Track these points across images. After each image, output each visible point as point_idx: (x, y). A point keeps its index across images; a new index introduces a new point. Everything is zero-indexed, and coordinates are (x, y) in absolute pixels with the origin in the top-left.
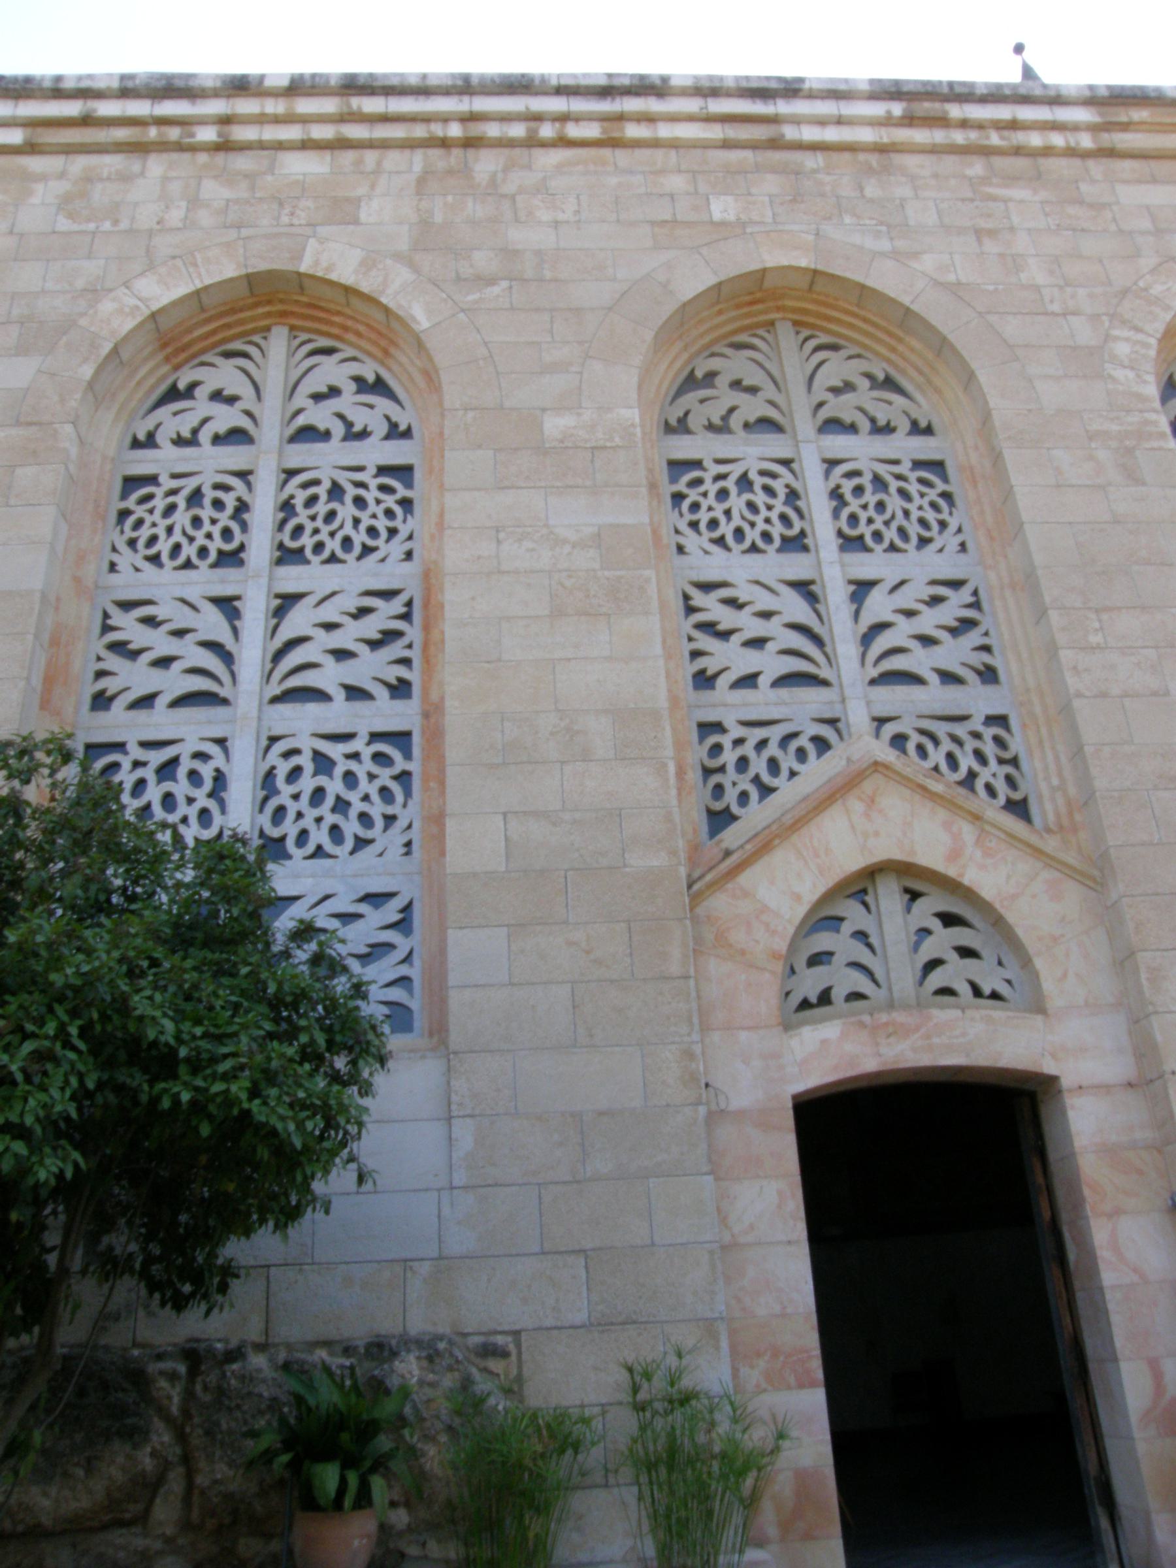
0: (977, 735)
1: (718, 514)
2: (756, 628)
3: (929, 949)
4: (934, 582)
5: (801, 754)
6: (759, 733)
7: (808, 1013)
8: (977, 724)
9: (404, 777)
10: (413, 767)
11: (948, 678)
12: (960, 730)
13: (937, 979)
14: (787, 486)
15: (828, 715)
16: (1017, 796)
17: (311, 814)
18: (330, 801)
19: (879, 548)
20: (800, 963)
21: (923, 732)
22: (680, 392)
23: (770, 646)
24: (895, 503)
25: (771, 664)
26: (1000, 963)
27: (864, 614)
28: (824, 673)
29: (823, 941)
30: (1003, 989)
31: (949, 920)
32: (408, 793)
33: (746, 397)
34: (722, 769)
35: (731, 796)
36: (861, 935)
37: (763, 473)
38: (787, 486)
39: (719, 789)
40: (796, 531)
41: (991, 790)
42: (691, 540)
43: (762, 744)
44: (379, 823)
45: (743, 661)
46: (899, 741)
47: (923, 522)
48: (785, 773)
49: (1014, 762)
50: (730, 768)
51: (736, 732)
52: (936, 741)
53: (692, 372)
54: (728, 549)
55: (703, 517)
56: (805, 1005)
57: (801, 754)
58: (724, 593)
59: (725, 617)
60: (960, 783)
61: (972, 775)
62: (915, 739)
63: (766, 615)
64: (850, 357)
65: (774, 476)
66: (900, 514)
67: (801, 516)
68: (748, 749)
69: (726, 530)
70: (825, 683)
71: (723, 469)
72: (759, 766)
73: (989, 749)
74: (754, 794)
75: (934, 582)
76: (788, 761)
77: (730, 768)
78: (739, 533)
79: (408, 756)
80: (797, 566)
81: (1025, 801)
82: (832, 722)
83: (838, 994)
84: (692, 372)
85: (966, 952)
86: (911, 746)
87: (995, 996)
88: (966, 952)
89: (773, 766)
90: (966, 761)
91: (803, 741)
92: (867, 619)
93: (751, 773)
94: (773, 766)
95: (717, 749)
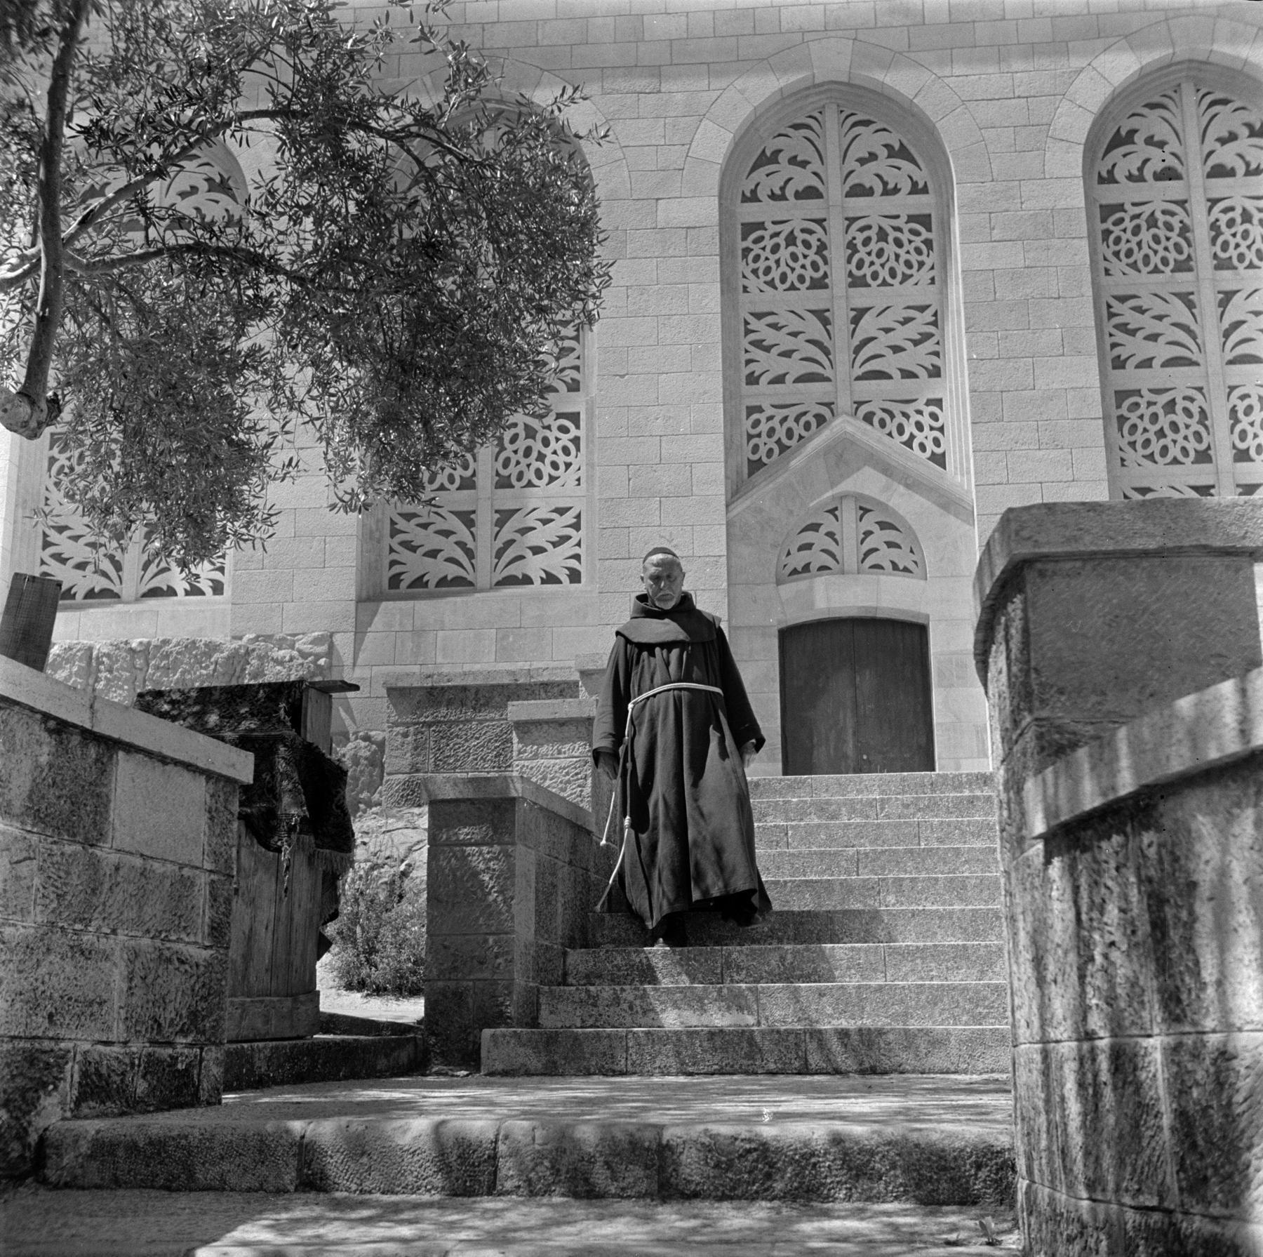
0: (919, 412)
1: (772, 263)
2: (788, 343)
3: (870, 543)
4: (909, 307)
5: (807, 426)
6: (785, 412)
7: (795, 576)
8: (920, 405)
9: (576, 441)
10: (581, 433)
11: (908, 374)
12: (910, 409)
13: (871, 560)
14: (819, 240)
15: (826, 400)
16: (938, 451)
17: (524, 461)
18: (534, 454)
19: (874, 284)
20: (794, 550)
21: (884, 410)
22: (753, 169)
23: (795, 355)
24: (890, 248)
25: (796, 367)
26: (912, 551)
27: (858, 330)
28: (828, 373)
29: (809, 537)
30: (911, 566)
31: (884, 525)
32: (578, 449)
33: (799, 169)
34: (759, 435)
35: (763, 452)
36: (831, 535)
37: (803, 231)
38: (819, 240)
39: (756, 449)
40: (821, 273)
41: (923, 447)
42: (752, 283)
43: (785, 419)
44: (562, 467)
45: (775, 365)
46: (868, 418)
47: (908, 264)
48: (796, 437)
49: (941, 429)
50: (764, 435)
51: (770, 411)
52: (892, 416)
53: (764, 151)
54: (776, 288)
55: (762, 265)
56: (795, 572)
57: (807, 426)
58: (770, 319)
59: (770, 336)
60: (904, 443)
61: (912, 437)
62: (880, 414)
63: (795, 334)
64: (877, 131)
65: (811, 232)
66: (893, 257)
67: (826, 262)
68: (775, 423)
69: (775, 274)
70: (828, 380)
71: (778, 228)
72: (781, 433)
73: (926, 421)
74: (777, 451)
75: (909, 307)
76: (798, 430)
77: (764, 435)
78: (783, 278)
79: (578, 427)
80: (818, 299)
81: (944, 454)
82: (828, 405)
83: (813, 567)
84: (764, 151)
85: (890, 545)
86: (876, 420)
87: (906, 570)
88: (890, 545)
89: (790, 434)
90: (910, 428)
91: (809, 417)
92: (860, 336)
93: (775, 438)
94: (790, 434)
95: (756, 423)
